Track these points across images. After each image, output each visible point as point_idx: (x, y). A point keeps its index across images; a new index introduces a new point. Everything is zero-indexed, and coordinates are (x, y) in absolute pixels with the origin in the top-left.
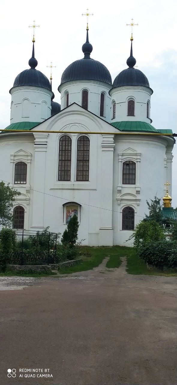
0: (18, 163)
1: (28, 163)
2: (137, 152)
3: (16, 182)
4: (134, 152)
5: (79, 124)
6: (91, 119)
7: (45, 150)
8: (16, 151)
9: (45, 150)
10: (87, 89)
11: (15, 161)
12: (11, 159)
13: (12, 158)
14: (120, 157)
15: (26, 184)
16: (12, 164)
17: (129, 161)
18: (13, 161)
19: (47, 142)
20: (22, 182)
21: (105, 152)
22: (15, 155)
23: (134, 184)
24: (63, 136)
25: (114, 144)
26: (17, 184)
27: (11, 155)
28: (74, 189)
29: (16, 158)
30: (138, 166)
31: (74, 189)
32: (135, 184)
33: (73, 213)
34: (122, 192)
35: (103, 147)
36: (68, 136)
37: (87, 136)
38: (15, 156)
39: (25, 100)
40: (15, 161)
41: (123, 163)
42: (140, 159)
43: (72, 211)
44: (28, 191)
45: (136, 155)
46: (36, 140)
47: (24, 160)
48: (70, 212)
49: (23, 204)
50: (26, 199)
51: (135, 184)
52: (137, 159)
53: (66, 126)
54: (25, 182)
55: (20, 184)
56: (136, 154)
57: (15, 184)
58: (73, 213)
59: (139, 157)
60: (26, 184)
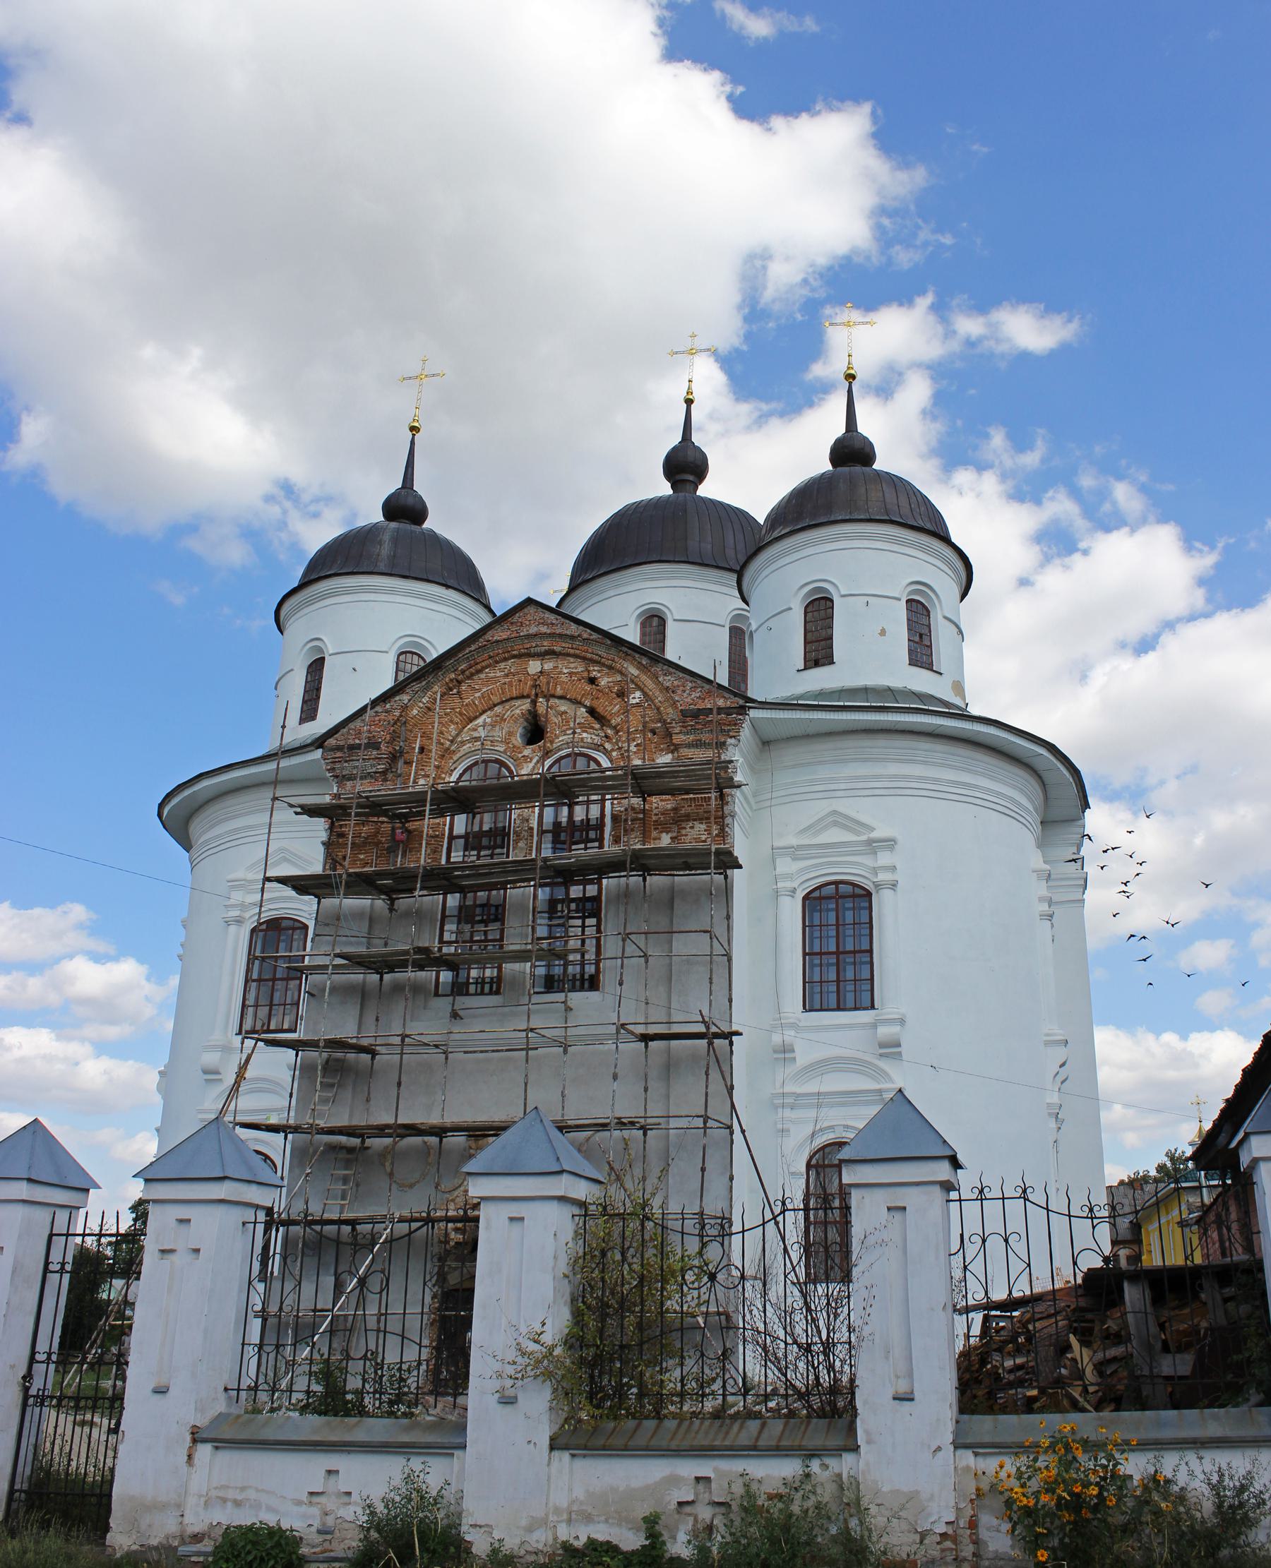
2: (874, 835)
4: (858, 833)
14: (785, 866)
17: (836, 883)
23: (865, 1009)
30: (886, 908)
32: (873, 1007)
34: (798, 1054)
40: (247, 915)
41: (805, 898)
42: (893, 869)
45: (874, 846)
51: (873, 1007)
52: (875, 871)
56: (870, 842)
59: (884, 859)
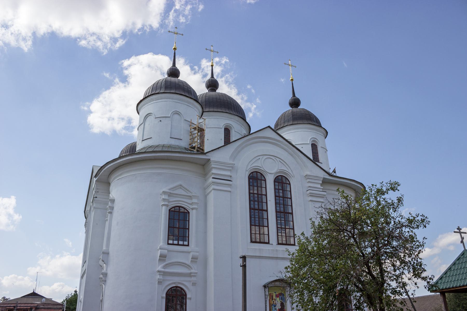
0: (174, 207)
1: (193, 209)
3: (171, 242)
5: (277, 158)
6: (290, 154)
7: (229, 189)
8: (169, 187)
9: (229, 189)
10: (232, 127)
11: (170, 204)
12: (164, 200)
13: (166, 197)
15: (188, 245)
16: (164, 207)
18: (166, 203)
19: (231, 176)
20: (181, 243)
21: (314, 202)
22: (171, 193)
24: (252, 173)
25: (325, 193)
26: (173, 244)
27: (164, 193)
28: (277, 258)
29: (172, 199)
31: (277, 258)
33: (278, 299)
35: (312, 195)
36: (262, 174)
37: (287, 177)
38: (170, 195)
39: (177, 113)
40: (170, 204)
43: (277, 296)
44: (194, 259)
46: (214, 171)
47: (185, 203)
48: (274, 297)
49: (184, 283)
50: (191, 273)
53: (258, 158)
54: (186, 243)
55: (178, 245)
57: (168, 244)
58: (278, 299)
60: (188, 245)
